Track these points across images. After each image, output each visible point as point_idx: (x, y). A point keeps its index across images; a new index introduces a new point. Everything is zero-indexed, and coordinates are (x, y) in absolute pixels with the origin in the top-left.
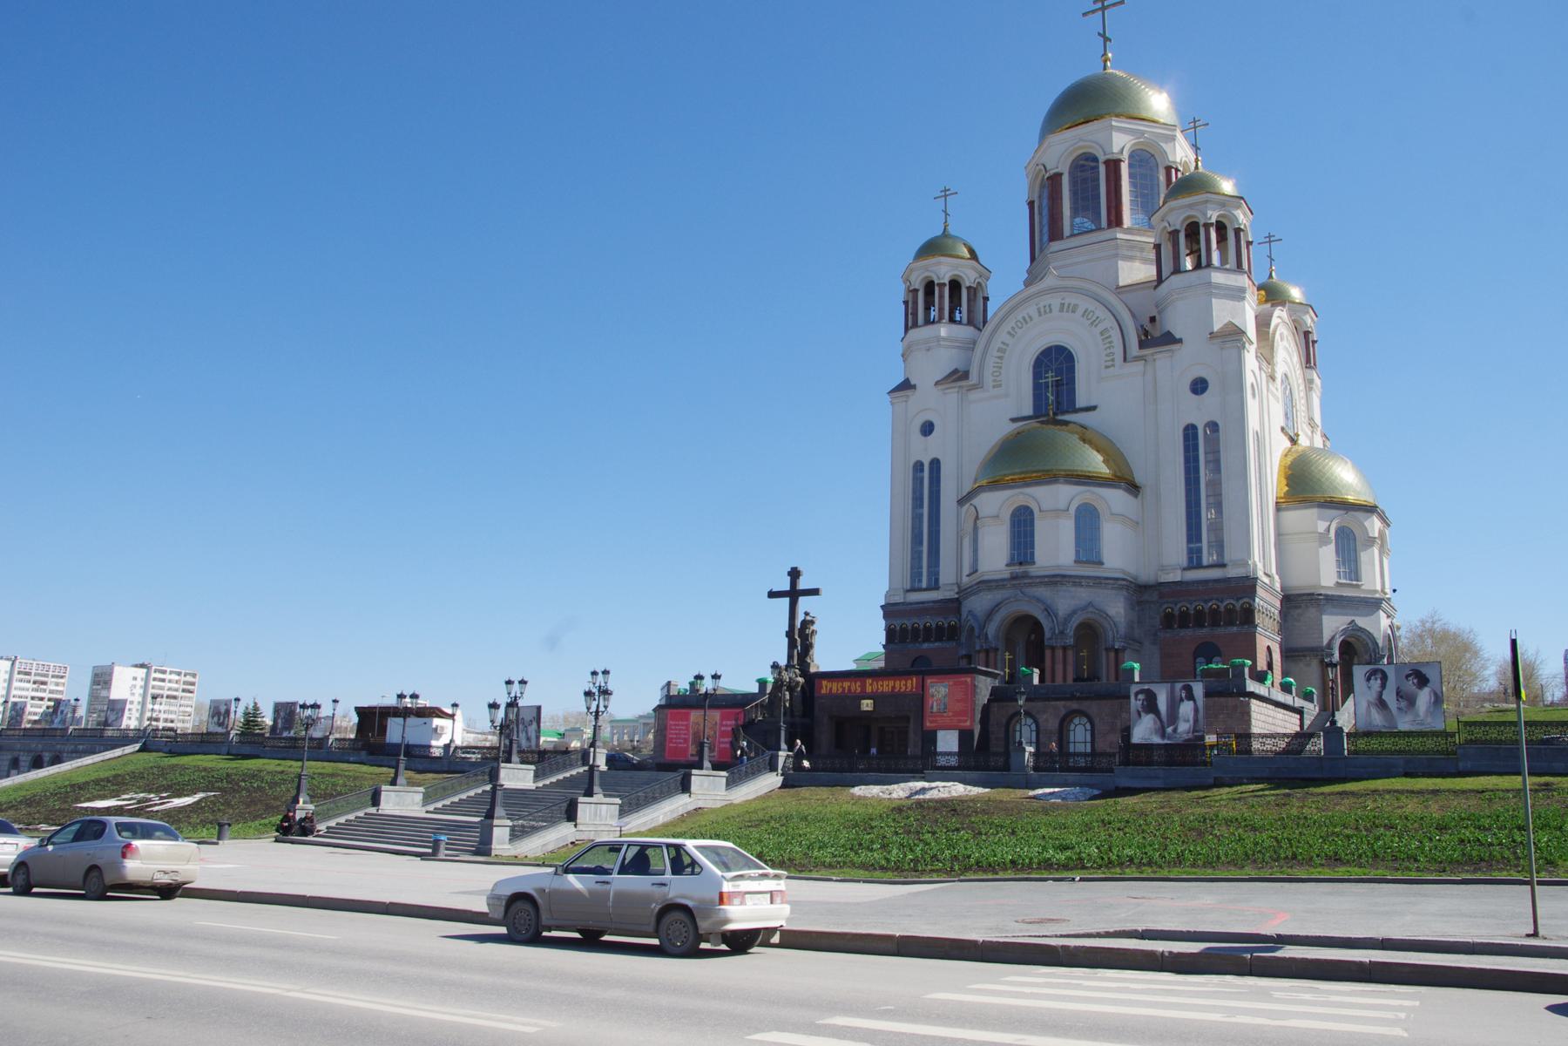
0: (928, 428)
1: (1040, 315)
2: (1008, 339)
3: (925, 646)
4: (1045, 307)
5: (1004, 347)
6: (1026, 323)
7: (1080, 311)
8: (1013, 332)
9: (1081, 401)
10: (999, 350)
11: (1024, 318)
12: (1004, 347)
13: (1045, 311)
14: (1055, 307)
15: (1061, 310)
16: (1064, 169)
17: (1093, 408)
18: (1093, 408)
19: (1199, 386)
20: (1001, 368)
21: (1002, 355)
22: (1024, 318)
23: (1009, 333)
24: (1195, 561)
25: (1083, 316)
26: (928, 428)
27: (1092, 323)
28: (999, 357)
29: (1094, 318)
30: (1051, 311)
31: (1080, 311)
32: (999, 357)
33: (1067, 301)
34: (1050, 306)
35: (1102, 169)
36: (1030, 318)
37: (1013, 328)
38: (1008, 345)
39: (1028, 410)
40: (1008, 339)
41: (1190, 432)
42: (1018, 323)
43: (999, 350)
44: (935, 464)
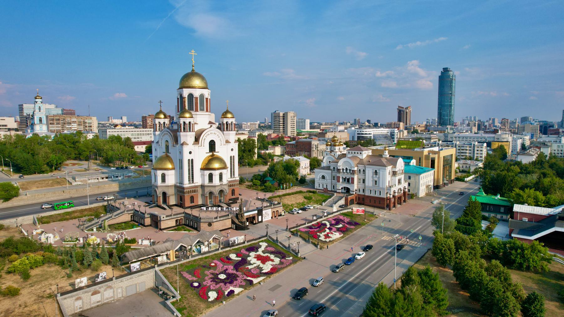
0: (190, 153)
2: (205, 138)
3: (193, 194)
7: (217, 134)
9: (216, 151)
10: (204, 140)
14: (213, 133)
16: (199, 97)
19: (232, 150)
24: (231, 177)
26: (190, 153)
31: (217, 134)
39: (208, 151)
40: (205, 138)
41: (231, 157)
44: (192, 160)
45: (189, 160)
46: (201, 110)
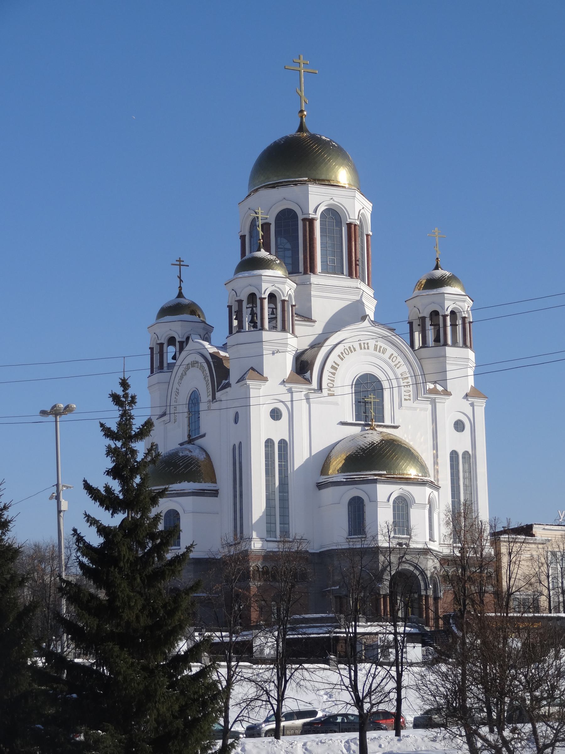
1: (361, 349)
2: (338, 361)
4: (364, 343)
5: (337, 366)
6: (352, 352)
8: (342, 356)
9: (387, 422)
10: (333, 367)
11: (350, 348)
12: (337, 366)
13: (365, 348)
15: (375, 349)
17: (396, 427)
18: (396, 427)
20: (333, 381)
21: (334, 371)
22: (350, 348)
23: (339, 356)
25: (389, 358)
27: (396, 365)
28: (332, 373)
29: (397, 362)
30: (368, 348)
32: (332, 373)
33: (379, 344)
34: (368, 344)
35: (344, 230)
36: (355, 350)
37: (342, 353)
38: (338, 365)
40: (338, 361)
41: (454, 455)
42: (345, 350)
43: (333, 367)
45: (269, 443)
46: (325, 270)
